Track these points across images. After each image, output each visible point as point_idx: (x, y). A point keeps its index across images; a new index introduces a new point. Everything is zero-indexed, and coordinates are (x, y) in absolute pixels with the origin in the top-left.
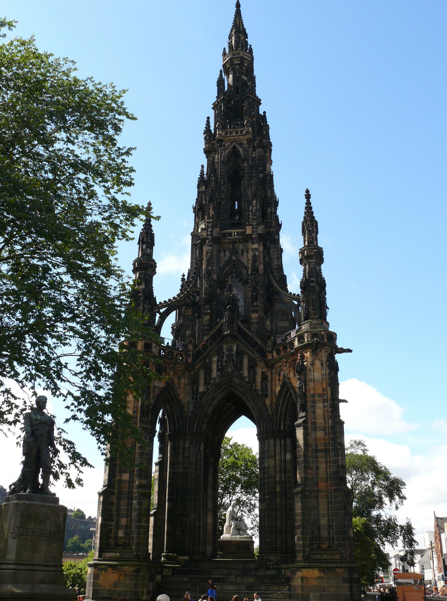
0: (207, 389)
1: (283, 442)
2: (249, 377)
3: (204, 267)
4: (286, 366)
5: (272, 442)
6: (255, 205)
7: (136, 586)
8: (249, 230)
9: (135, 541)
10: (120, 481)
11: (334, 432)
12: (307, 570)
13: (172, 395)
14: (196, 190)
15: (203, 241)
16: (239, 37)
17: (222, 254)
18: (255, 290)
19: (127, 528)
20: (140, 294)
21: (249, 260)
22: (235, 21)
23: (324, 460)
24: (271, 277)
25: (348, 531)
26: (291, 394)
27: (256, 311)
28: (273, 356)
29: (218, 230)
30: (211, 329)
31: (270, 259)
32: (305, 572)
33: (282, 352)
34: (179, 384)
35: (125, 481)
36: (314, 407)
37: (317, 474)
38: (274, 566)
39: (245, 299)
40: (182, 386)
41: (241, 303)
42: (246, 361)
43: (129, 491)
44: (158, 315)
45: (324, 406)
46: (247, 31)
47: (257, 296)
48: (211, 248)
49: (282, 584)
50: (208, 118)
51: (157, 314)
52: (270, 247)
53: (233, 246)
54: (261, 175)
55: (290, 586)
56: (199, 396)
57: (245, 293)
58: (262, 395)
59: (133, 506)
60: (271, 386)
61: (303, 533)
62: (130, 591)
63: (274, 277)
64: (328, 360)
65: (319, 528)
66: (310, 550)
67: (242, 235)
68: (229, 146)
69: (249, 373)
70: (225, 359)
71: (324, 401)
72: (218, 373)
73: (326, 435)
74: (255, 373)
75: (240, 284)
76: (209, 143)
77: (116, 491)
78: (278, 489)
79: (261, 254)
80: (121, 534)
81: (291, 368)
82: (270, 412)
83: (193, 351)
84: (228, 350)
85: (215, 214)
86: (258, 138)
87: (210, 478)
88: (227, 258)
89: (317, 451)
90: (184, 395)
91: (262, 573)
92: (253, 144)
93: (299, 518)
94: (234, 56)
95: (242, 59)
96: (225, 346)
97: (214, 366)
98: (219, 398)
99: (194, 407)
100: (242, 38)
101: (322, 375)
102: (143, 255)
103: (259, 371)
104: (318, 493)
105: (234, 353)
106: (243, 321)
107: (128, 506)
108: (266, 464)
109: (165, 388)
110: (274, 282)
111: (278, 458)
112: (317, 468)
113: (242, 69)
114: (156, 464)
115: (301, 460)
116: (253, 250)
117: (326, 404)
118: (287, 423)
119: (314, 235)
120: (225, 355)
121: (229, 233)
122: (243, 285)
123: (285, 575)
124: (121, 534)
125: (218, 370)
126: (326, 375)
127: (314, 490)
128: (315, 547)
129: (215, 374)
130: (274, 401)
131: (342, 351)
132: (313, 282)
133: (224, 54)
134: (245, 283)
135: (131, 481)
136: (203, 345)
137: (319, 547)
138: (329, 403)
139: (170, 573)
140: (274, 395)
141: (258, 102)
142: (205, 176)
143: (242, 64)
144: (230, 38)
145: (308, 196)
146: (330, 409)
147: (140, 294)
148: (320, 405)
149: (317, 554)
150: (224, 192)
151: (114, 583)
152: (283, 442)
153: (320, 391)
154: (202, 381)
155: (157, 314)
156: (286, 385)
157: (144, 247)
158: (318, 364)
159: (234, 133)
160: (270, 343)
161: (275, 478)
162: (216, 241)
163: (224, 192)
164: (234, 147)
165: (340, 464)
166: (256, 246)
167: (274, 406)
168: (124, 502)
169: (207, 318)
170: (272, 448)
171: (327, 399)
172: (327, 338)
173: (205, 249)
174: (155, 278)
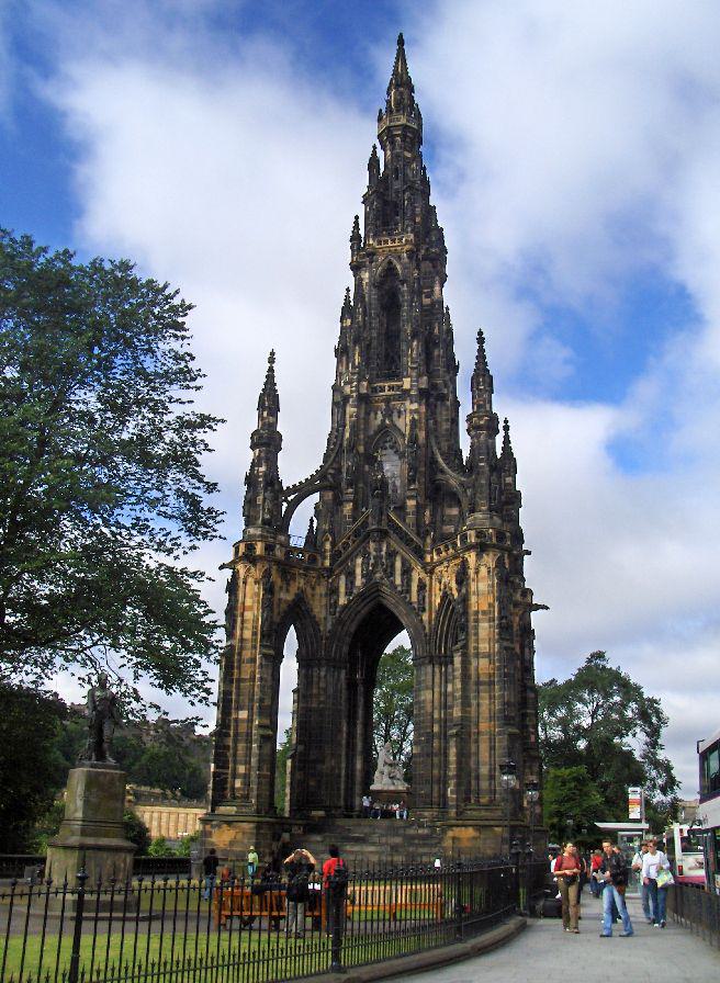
0: (349, 601)
2: (402, 585)
5: (429, 669)
9: (255, 793)
10: (236, 720)
15: (346, 399)
20: (261, 479)
22: (396, 67)
28: (432, 558)
30: (355, 520)
31: (436, 423)
34: (313, 596)
35: (243, 720)
36: (476, 628)
42: (398, 564)
44: (285, 504)
50: (357, 218)
52: (436, 406)
53: (387, 406)
54: (427, 301)
65: (478, 778)
70: (372, 561)
71: (491, 620)
75: (397, 458)
78: (436, 729)
80: (238, 784)
82: (427, 631)
86: (425, 247)
88: (378, 422)
89: (478, 683)
91: (411, 832)
93: (453, 766)
94: (392, 124)
95: (405, 127)
96: (372, 545)
102: (264, 425)
103: (417, 574)
105: (383, 553)
108: (423, 698)
111: (437, 689)
116: (412, 412)
122: (400, 458)
124: (238, 784)
126: (493, 586)
129: (359, 582)
132: (481, 460)
135: (250, 720)
138: (496, 622)
139: (301, 831)
144: (389, 94)
147: (261, 479)
153: (486, 608)
154: (342, 589)
157: (265, 414)
158: (483, 570)
160: (429, 541)
162: (364, 400)
173: (350, 410)
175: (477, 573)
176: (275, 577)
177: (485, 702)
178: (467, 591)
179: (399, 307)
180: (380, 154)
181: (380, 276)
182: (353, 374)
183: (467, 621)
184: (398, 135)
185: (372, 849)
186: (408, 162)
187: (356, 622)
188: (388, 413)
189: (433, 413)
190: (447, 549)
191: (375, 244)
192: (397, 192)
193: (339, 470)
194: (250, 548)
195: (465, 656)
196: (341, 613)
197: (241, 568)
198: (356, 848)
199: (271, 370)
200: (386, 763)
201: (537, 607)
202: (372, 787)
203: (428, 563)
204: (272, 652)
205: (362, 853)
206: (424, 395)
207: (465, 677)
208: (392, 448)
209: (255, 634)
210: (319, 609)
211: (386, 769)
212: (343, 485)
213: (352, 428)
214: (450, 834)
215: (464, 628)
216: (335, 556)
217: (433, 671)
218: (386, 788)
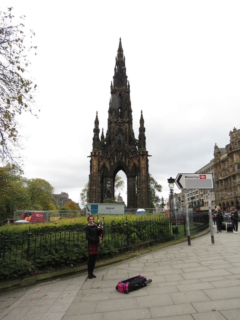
2: (125, 161)
3: (112, 130)
6: (126, 112)
14: (109, 106)
15: (112, 122)
17: (117, 126)
27: (127, 144)
35: (94, 189)
36: (142, 170)
42: (124, 157)
46: (123, 50)
61: (139, 201)
70: (118, 156)
78: (132, 190)
88: (118, 127)
89: (143, 181)
95: (122, 61)
99: (111, 169)
103: (127, 160)
108: (129, 184)
109: (103, 164)
111: (132, 182)
118: (135, 173)
125: (117, 159)
128: (142, 204)
131: (150, 156)
134: (123, 135)
135: (96, 189)
141: (127, 77)
143: (122, 63)
145: (142, 112)
154: (112, 162)
157: (96, 125)
160: (130, 153)
164: (120, 93)
166: (126, 125)
169: (113, 145)
170: (131, 180)
173: (113, 125)
177: (144, 186)
180: (117, 68)
186: (123, 70)
187: (115, 169)
188: (120, 126)
189: (130, 126)
190: (134, 154)
194: (95, 153)
197: (93, 158)
199: (97, 115)
206: (128, 122)
209: (96, 171)
210: (108, 166)
213: (113, 128)
215: (140, 171)
217: (131, 179)
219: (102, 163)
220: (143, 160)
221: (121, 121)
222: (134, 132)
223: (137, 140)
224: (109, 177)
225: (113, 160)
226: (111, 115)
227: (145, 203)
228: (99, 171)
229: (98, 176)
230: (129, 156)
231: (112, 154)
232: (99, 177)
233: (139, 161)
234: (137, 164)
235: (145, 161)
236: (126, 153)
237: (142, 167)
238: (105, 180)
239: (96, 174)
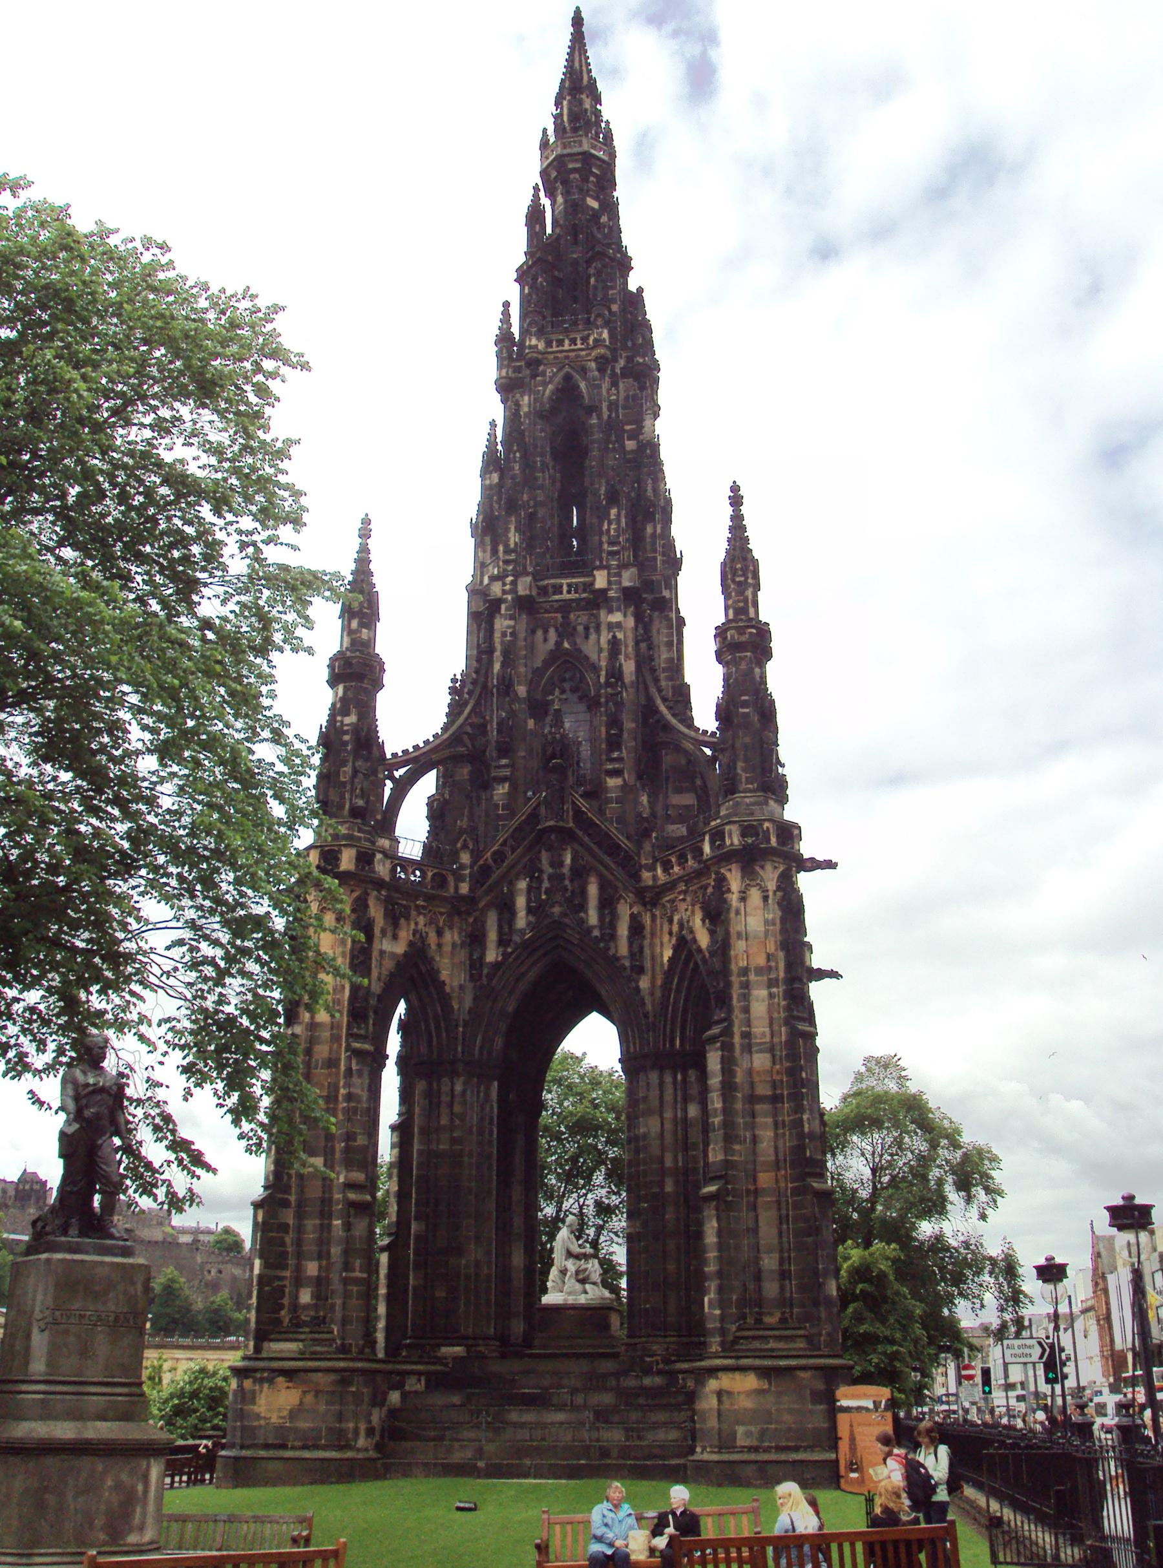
0: (505, 954)
1: (679, 1077)
2: (601, 927)
3: (497, 667)
4: (684, 900)
6: (615, 521)
7: (340, 1417)
8: (601, 580)
9: (338, 1315)
10: (301, 1177)
11: (793, 1056)
12: (730, 1375)
13: (424, 970)
15: (494, 606)
16: (581, 102)
18: (614, 722)
19: (320, 1284)
20: (347, 738)
21: (600, 650)
22: (570, 60)
23: (770, 1120)
24: (653, 690)
25: (824, 1284)
26: (696, 963)
28: (655, 878)
29: (529, 579)
30: (513, 814)
31: (650, 648)
32: (725, 1381)
33: (676, 869)
34: (439, 945)
36: (746, 997)
37: (754, 1153)
38: (661, 1366)
39: (592, 741)
40: (447, 949)
41: (585, 750)
42: (593, 890)
43: (323, 1200)
44: (389, 784)
45: (771, 996)
46: (600, 86)
47: (620, 735)
48: (512, 623)
49: (678, 1407)
50: (506, 305)
51: (388, 782)
52: (650, 617)
54: (630, 445)
55: (694, 1412)
56: (485, 971)
57: (593, 729)
58: (632, 967)
59: (334, 1233)
60: (652, 946)
61: (720, 1290)
62: (329, 1429)
63: (660, 690)
64: (779, 888)
65: (758, 1277)
66: (739, 1329)
67: (584, 591)
68: (555, 374)
69: (601, 918)
70: (546, 884)
71: (771, 983)
72: (531, 918)
73: (774, 1063)
74: (614, 917)
75: (582, 707)
76: (508, 366)
77: (293, 1198)
78: (669, 1188)
79: (630, 635)
81: (697, 907)
82: (649, 1007)
83: (472, 867)
84: (552, 865)
85: (522, 540)
87: (518, 1161)
89: (752, 1099)
90: (450, 971)
91: (630, 1382)
92: (613, 369)
93: (712, 1255)
94: (566, 151)
95: (587, 157)
96: (545, 857)
97: (521, 902)
98: (532, 974)
99: (475, 999)
100: (587, 104)
101: (766, 922)
102: (353, 642)
103: (624, 911)
104: (756, 1198)
105: (566, 870)
106: (586, 795)
107: (322, 1231)
109: (405, 954)
110: (659, 702)
111: (668, 1115)
112: (755, 1140)
113: (587, 181)
114: (393, 1128)
115: (717, 1120)
116: (611, 626)
117: (774, 990)
119: (749, 593)
120: (545, 877)
121: (554, 586)
122: (589, 708)
123: (684, 1387)
124: (305, 1297)
125: (529, 911)
127: (748, 1191)
128: (750, 1321)
129: (521, 920)
130: (659, 982)
131: (814, 865)
132: (745, 704)
133: (544, 144)
134: (593, 704)
136: (496, 853)
137: (759, 1321)
139: (421, 1387)
140: (658, 969)
141: (624, 264)
142: (499, 447)
143: (585, 172)
144: (558, 103)
145: (736, 500)
146: (783, 1003)
147: (347, 738)
148: (760, 994)
149: (754, 1338)
150: (542, 487)
151: (291, 1411)
152: (679, 1077)
153: (761, 961)
154: (492, 936)
155: (388, 782)
156: (684, 944)
157: (355, 624)
159: (567, 342)
161: (662, 1162)
163: (542, 487)
164: (568, 378)
165: (806, 1130)
166: (616, 617)
167: (658, 993)
168: (311, 1224)
169: (502, 790)
170: (654, 1093)
171: (777, 980)
172: (778, 837)
173: (502, 624)
174: (381, 696)
175: (743, 899)
176: (376, 912)
178: (727, 934)
179: (584, 452)
180: (545, 201)
181: (550, 398)
182: (506, 562)
183: (729, 985)
184: (575, 170)
185: (561, 1417)
188: (566, 631)
189: (647, 630)
190: (682, 860)
191: (541, 346)
192: (575, 263)
193: (482, 728)
195: (727, 1048)
196: (490, 977)
198: (529, 1417)
199: (364, 550)
200: (570, 1254)
201: (821, 974)
202: (546, 1299)
203: (647, 887)
204: (367, 1047)
205: (543, 1426)
206: (630, 597)
207: (728, 1087)
208: (574, 690)
211: (571, 1266)
212: (491, 752)
213: (506, 653)
214: (713, 1384)
215: (724, 1000)
216: (481, 875)
217: (662, 1083)
218: (571, 1300)
219: (394, 947)
220: (755, 895)
221: (573, 596)
222: (688, 679)
223: (702, 738)
224: (460, 1067)
225: (500, 927)
226: (494, 552)
227: (784, 1302)
228: (357, 1014)
229: (349, 1059)
230: (636, 877)
231: (486, 871)
232: (354, 1067)
233: (716, 914)
234: (703, 939)
235: (774, 913)
236: (613, 849)
237: (743, 963)
238: (429, 1094)
239: (335, 1039)
